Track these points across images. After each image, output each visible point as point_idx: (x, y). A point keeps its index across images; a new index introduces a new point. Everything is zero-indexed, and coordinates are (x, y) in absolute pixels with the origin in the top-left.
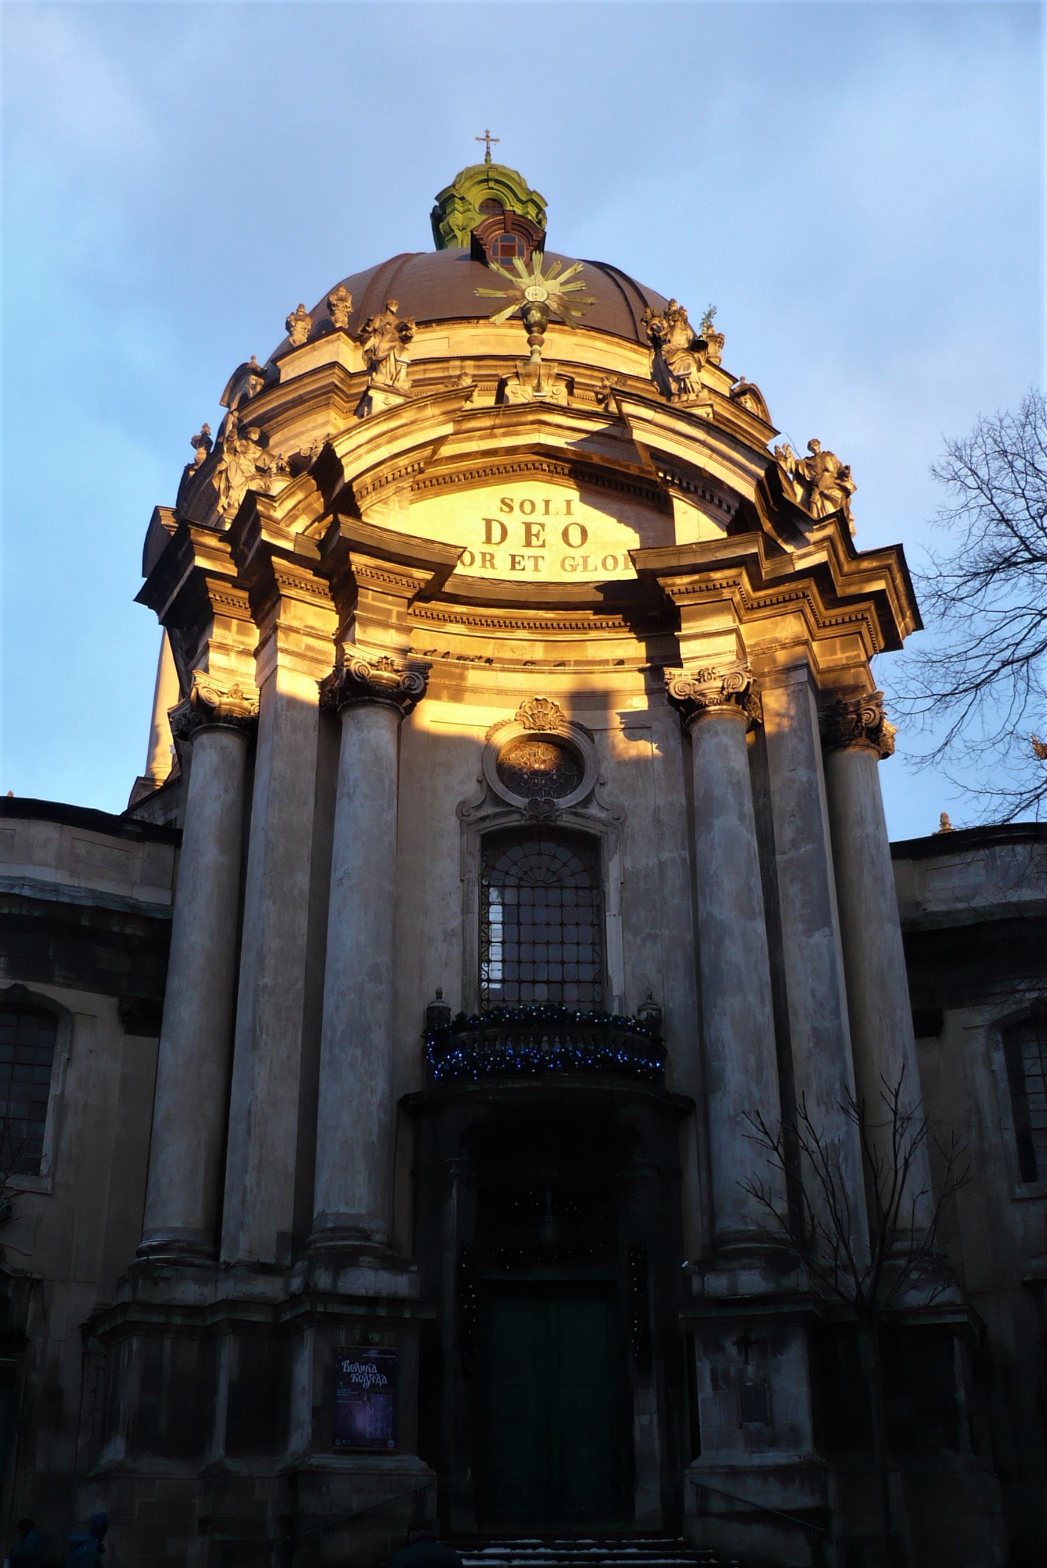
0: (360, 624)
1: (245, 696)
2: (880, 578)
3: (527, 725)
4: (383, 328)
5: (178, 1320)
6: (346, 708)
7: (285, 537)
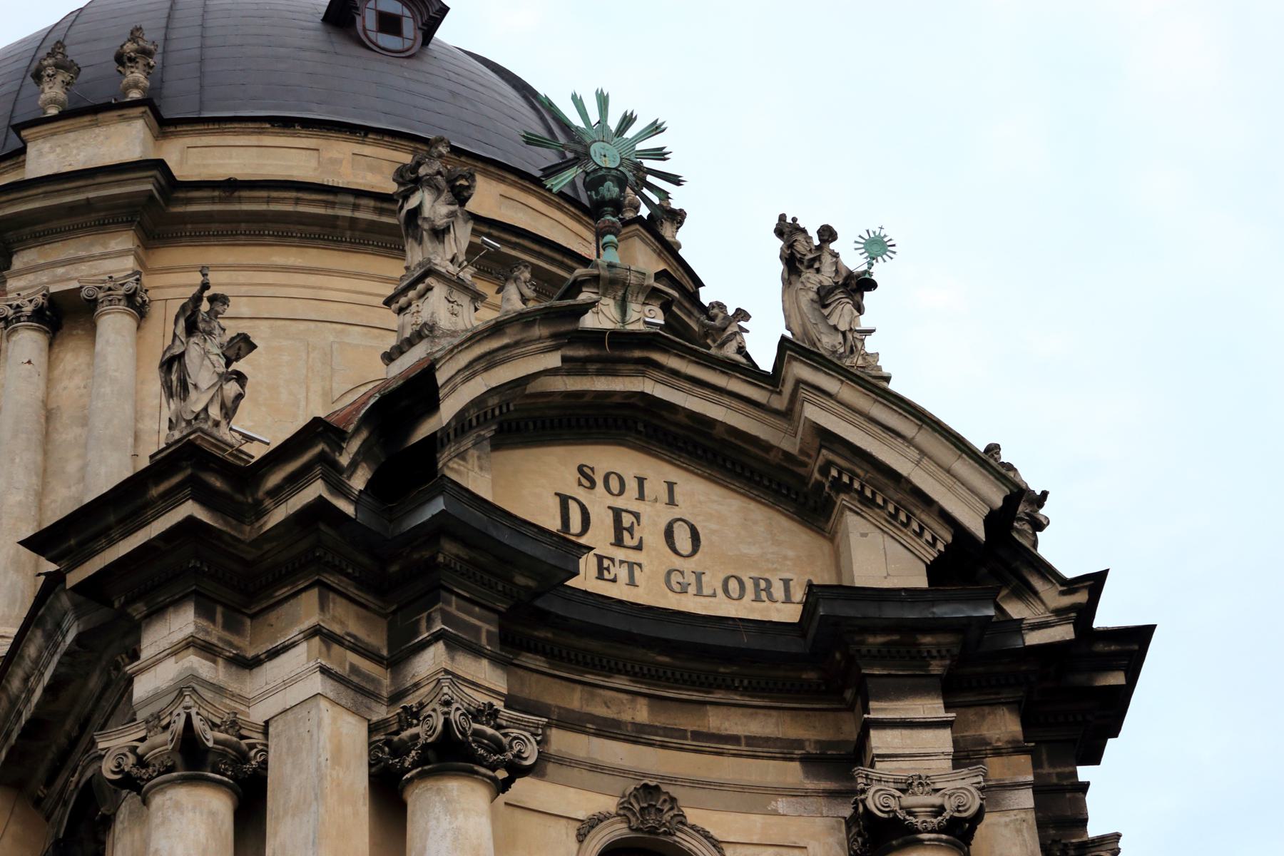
0: (446, 645)
1: (244, 732)
2: (1117, 669)
3: (634, 823)
4: (432, 176)
6: (422, 776)
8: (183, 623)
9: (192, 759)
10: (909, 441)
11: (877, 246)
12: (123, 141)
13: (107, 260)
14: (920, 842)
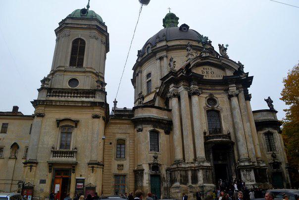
8: (172, 85)
9: (174, 96)
11: (227, 46)
12: (164, 43)
13: (164, 53)
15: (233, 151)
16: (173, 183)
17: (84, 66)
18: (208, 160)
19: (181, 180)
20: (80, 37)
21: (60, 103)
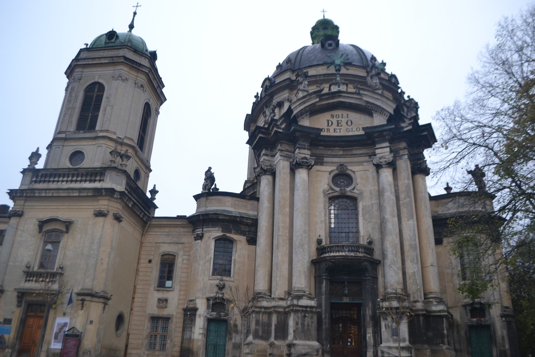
5: (263, 310)
7: (280, 128)
8: (264, 152)
9: (264, 172)
10: (380, 100)
12: (287, 75)
14: (382, 167)
15: (376, 278)
16: (247, 337)
17: (97, 128)
18: (318, 295)
19: (256, 331)
20: (96, 80)
21: (46, 193)
